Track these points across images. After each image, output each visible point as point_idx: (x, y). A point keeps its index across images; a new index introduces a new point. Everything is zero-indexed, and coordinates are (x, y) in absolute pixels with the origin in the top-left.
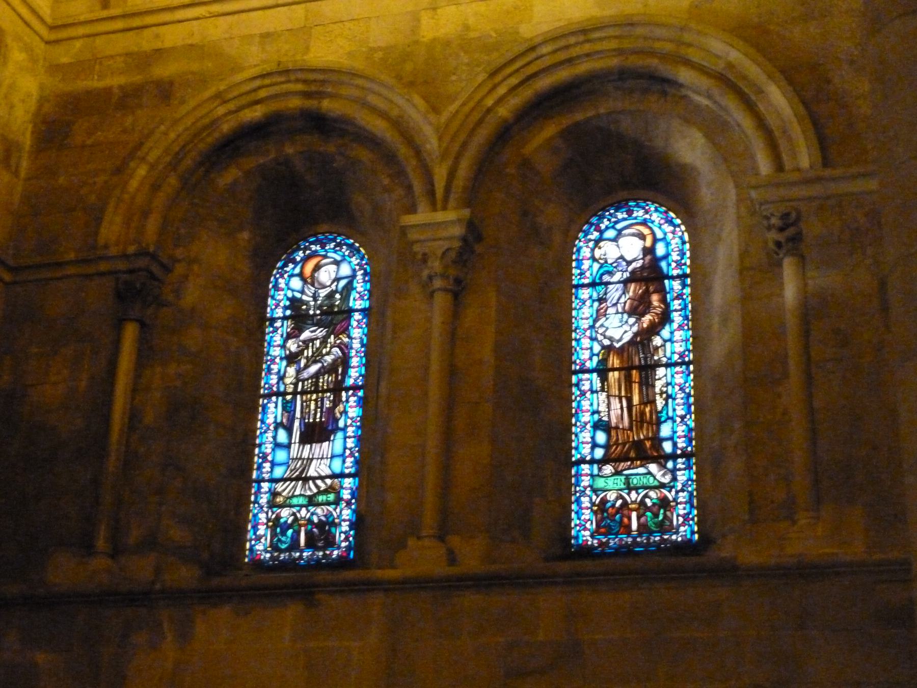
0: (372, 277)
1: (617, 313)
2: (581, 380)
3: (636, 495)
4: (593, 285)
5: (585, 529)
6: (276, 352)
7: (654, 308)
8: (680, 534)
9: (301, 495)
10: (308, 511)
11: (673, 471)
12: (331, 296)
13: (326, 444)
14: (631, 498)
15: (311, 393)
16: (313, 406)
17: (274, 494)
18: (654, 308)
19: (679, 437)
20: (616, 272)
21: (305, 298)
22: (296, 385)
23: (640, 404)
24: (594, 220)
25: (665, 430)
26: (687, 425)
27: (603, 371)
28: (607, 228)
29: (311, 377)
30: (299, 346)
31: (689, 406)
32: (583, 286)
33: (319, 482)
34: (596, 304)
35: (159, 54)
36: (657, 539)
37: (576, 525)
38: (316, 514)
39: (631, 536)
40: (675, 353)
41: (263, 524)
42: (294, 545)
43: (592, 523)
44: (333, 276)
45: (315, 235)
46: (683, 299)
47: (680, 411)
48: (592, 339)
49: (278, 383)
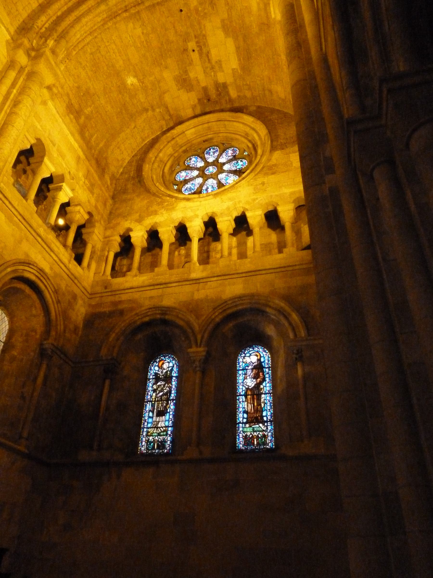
0: (179, 367)
1: (250, 378)
4: (243, 370)
5: (241, 444)
6: (150, 389)
9: (156, 432)
10: (158, 437)
11: (267, 426)
12: (167, 372)
13: (164, 417)
15: (160, 401)
16: (160, 405)
17: (148, 432)
19: (268, 416)
21: (159, 373)
22: (155, 399)
24: (243, 351)
25: (264, 414)
27: (246, 395)
28: (247, 353)
29: (160, 396)
30: (157, 387)
31: (271, 406)
32: (240, 370)
33: (161, 429)
34: (244, 375)
35: (120, 302)
36: (262, 447)
37: (238, 443)
38: (160, 439)
41: (144, 441)
42: (153, 448)
44: (167, 366)
45: (162, 354)
47: (269, 408)
48: (243, 386)
49: (150, 398)
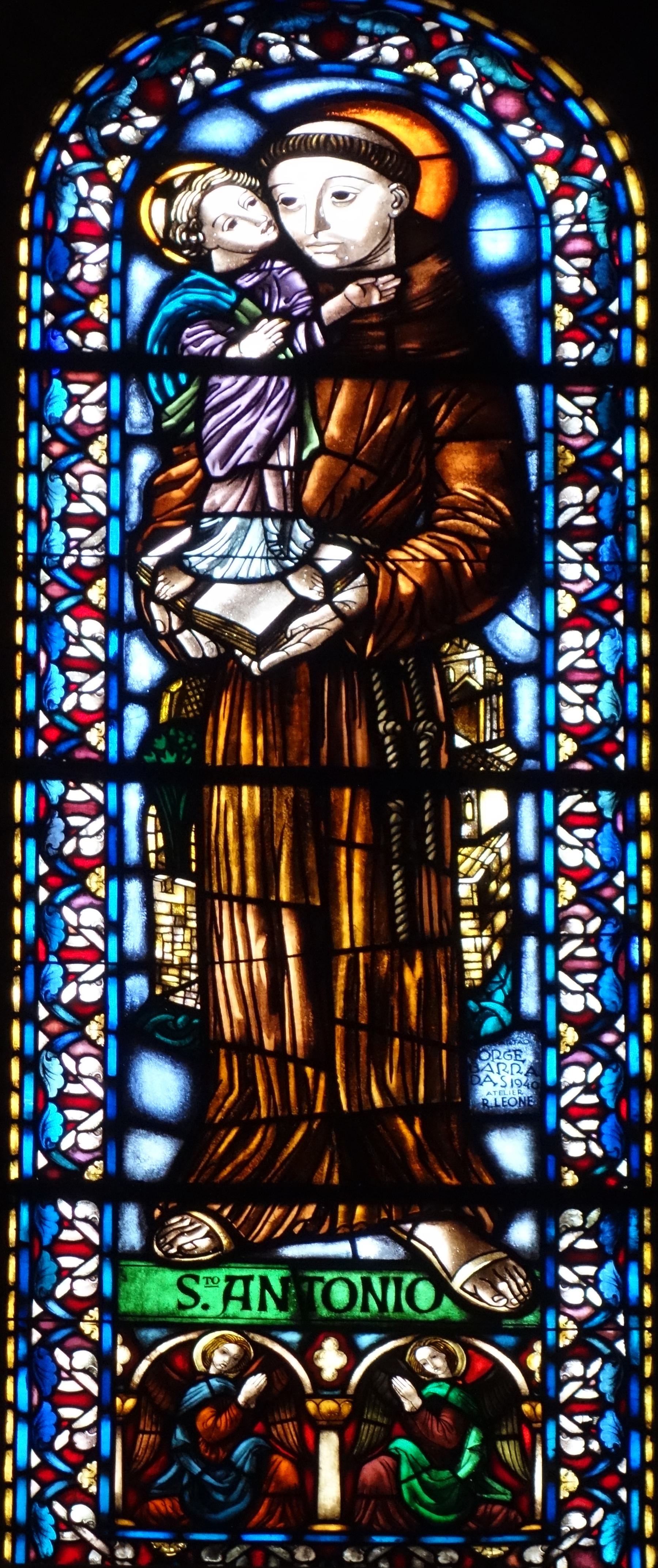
2: (63, 808)
3: (341, 1360)
7: (458, 511)
8: (567, 1544)
14: (314, 1372)
18: (458, 511)
19: (573, 1113)
20: (254, 321)
23: (372, 947)
26: (611, 1060)
37: (24, 1474)
39: (311, 1538)
40: (560, 726)
43: (106, 1469)
46: (617, 489)
